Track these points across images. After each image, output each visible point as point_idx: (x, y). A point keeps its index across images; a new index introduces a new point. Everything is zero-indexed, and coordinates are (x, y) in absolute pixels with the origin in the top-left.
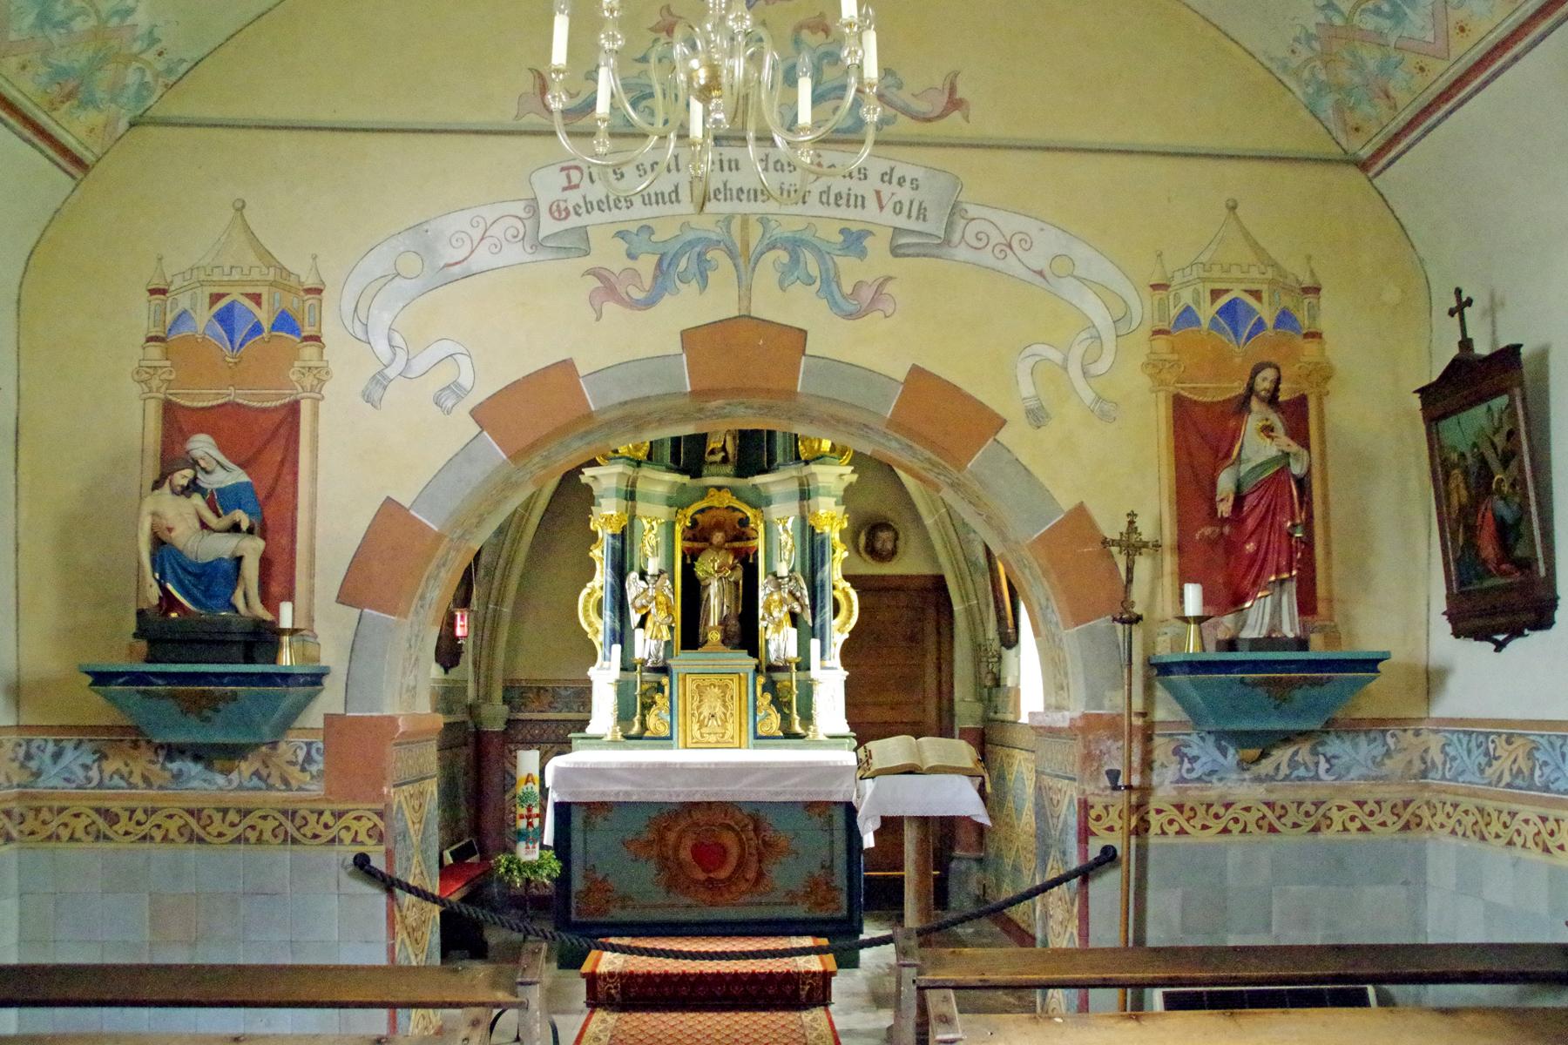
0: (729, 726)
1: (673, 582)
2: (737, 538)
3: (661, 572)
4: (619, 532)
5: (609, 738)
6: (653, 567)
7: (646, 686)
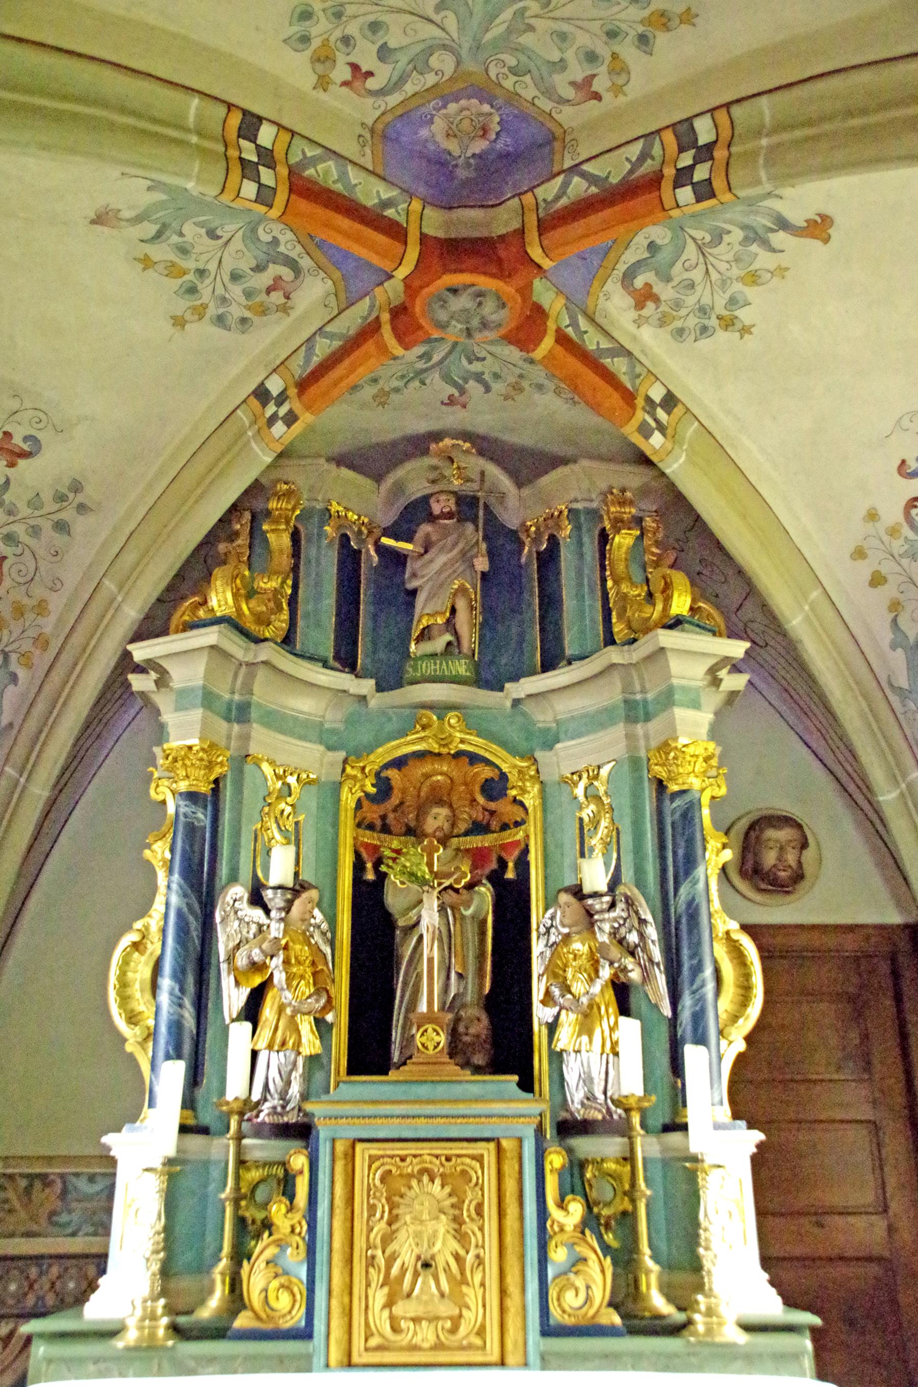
0: (472, 1295)
1: (332, 920)
2: (479, 828)
4: (205, 788)
5: (131, 1337)
6: (281, 868)
7: (254, 1175)
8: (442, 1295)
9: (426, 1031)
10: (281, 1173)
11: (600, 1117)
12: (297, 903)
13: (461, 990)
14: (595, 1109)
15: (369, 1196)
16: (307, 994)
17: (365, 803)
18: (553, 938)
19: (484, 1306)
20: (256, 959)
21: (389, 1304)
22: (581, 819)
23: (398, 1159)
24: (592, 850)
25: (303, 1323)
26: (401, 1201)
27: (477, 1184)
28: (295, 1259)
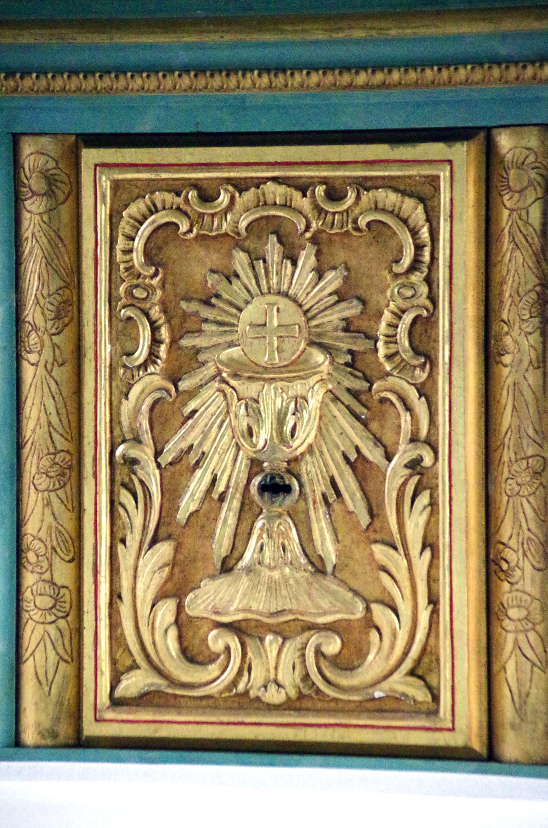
8: (318, 567)
19: (433, 601)
23: (192, 194)
26: (206, 313)
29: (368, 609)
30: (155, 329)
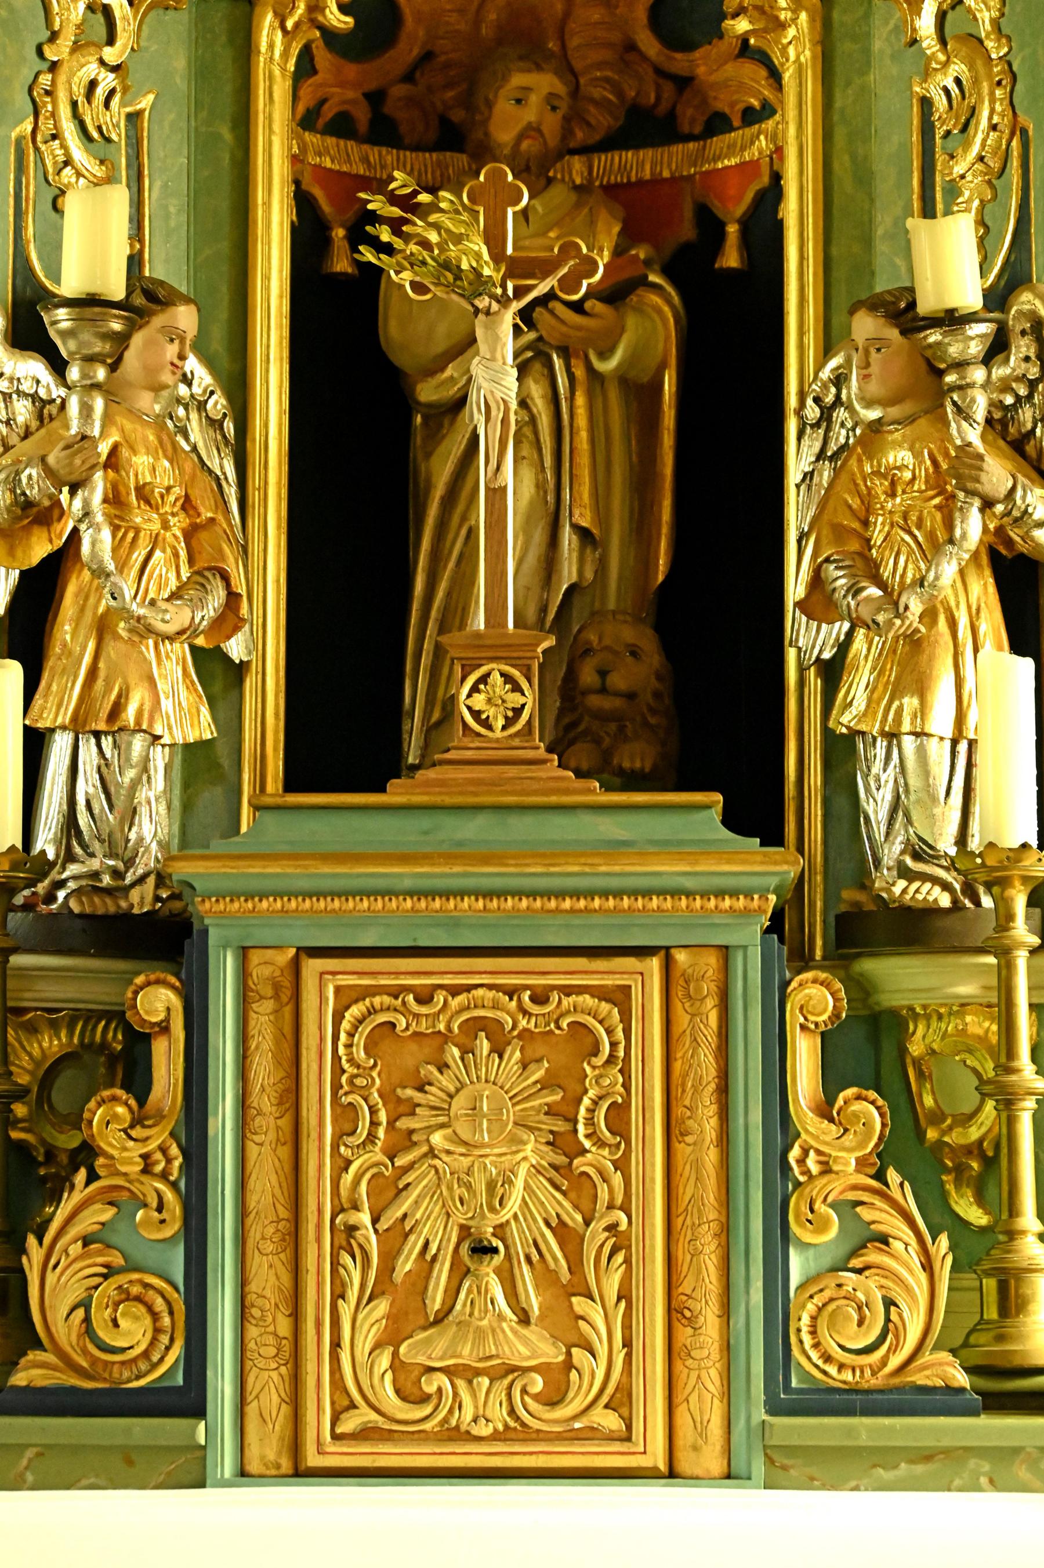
1: (238, 386)
3: (146, 298)
9: (484, 679)
10: (117, 1042)
11: (945, 901)
12: (138, 340)
13: (589, 575)
14: (935, 880)
15: (336, 1087)
16: (173, 584)
17: (323, 57)
18: (839, 436)
20: (33, 493)
21: (392, 1337)
22: (926, 103)
24: (953, 191)
25: (180, 1381)
26: (418, 1097)
27: (611, 1059)
28: (158, 1230)
29: (569, 1354)
30: (373, 1111)
